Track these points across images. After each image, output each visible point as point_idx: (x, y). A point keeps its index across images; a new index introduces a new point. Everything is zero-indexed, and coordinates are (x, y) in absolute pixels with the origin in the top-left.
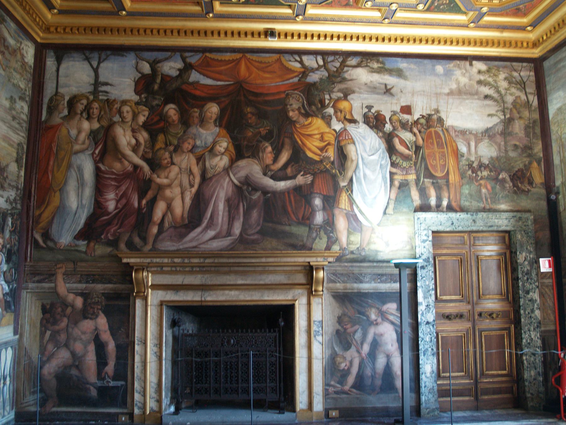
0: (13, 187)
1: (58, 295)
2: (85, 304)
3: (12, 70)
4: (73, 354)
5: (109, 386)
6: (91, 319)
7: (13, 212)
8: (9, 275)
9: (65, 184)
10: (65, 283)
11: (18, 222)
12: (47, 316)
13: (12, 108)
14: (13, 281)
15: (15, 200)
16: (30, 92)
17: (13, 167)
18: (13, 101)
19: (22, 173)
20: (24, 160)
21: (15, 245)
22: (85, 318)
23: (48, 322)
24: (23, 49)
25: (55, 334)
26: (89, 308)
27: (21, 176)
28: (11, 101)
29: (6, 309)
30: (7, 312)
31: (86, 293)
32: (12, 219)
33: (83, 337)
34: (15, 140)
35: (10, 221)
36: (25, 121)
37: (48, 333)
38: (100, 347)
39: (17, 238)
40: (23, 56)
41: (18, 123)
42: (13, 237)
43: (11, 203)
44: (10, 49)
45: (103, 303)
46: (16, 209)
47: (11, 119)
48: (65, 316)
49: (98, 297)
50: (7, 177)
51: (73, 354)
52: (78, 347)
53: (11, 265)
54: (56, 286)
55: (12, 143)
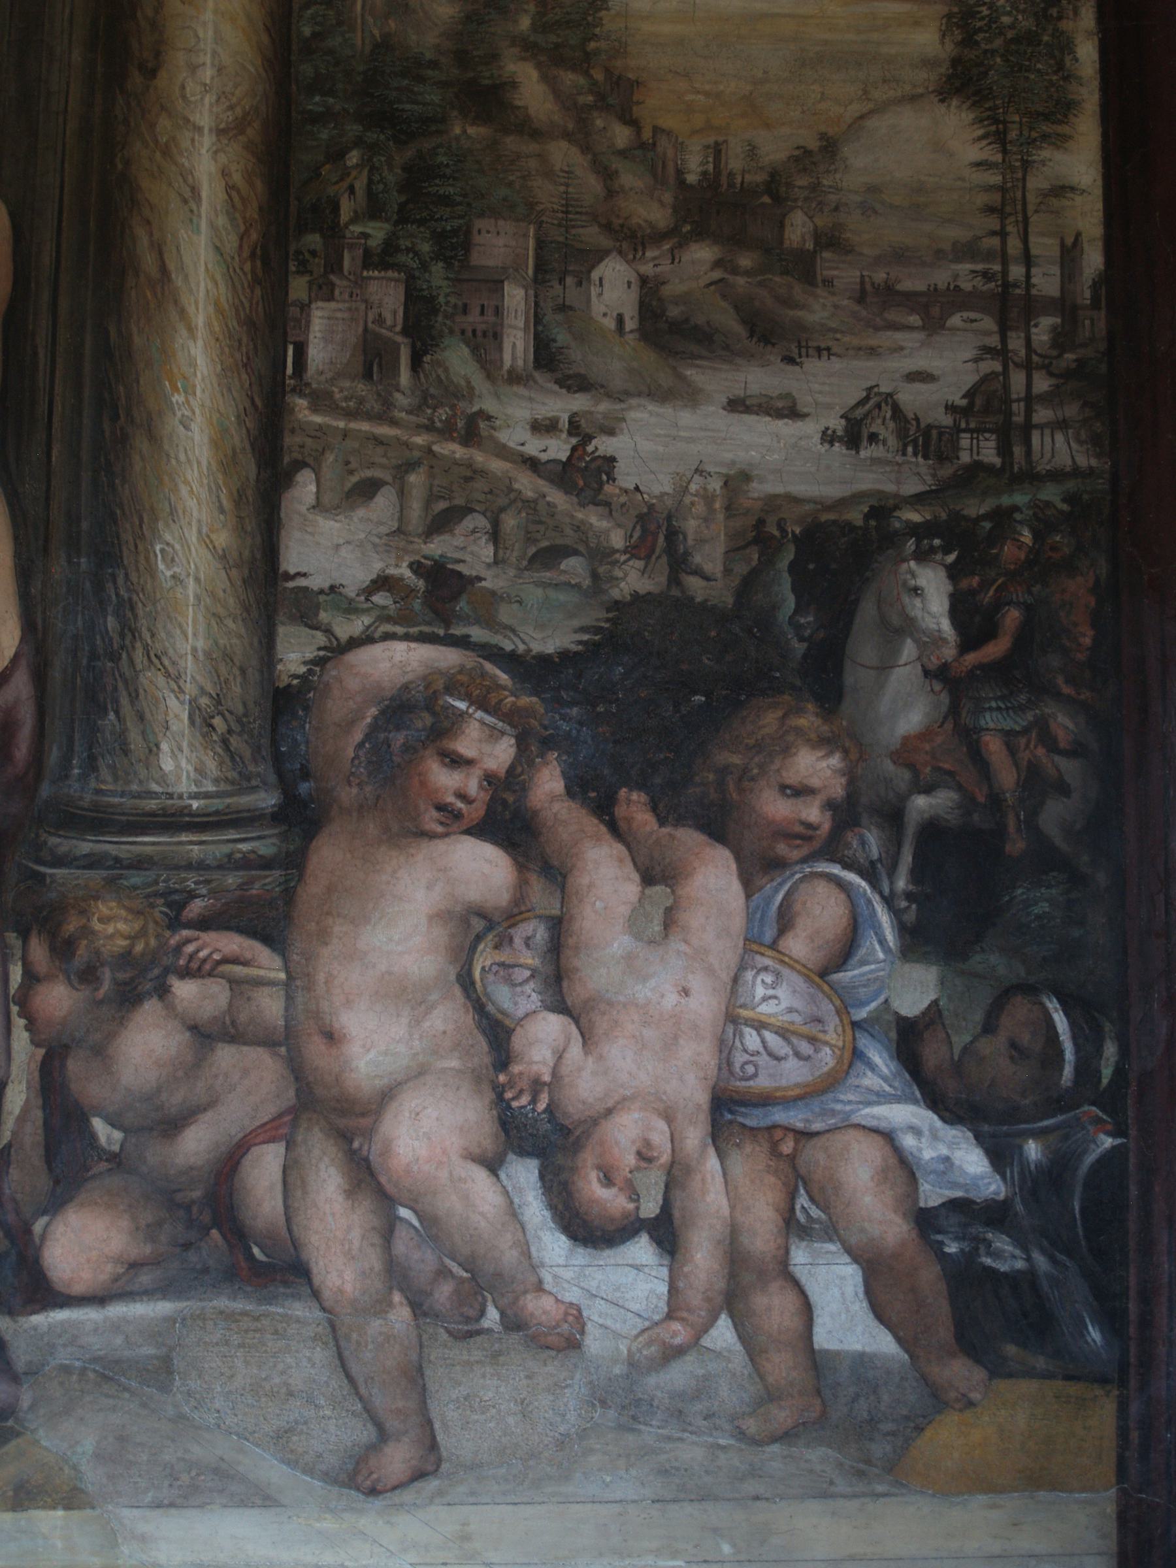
0: (933, 311)
7: (975, 507)
8: (993, 1047)
11: (1077, 592)
14: (1059, 1103)
15: (985, 406)
17: (929, 149)
19: (1077, 162)
20: (1087, 53)
21: (1036, 783)
27: (1062, 190)
29: (971, 1341)
30: (998, 1370)
32: (954, 573)
39: (1064, 724)
42: (989, 720)
46: (1030, 477)
50: (830, 240)
53: (993, 961)
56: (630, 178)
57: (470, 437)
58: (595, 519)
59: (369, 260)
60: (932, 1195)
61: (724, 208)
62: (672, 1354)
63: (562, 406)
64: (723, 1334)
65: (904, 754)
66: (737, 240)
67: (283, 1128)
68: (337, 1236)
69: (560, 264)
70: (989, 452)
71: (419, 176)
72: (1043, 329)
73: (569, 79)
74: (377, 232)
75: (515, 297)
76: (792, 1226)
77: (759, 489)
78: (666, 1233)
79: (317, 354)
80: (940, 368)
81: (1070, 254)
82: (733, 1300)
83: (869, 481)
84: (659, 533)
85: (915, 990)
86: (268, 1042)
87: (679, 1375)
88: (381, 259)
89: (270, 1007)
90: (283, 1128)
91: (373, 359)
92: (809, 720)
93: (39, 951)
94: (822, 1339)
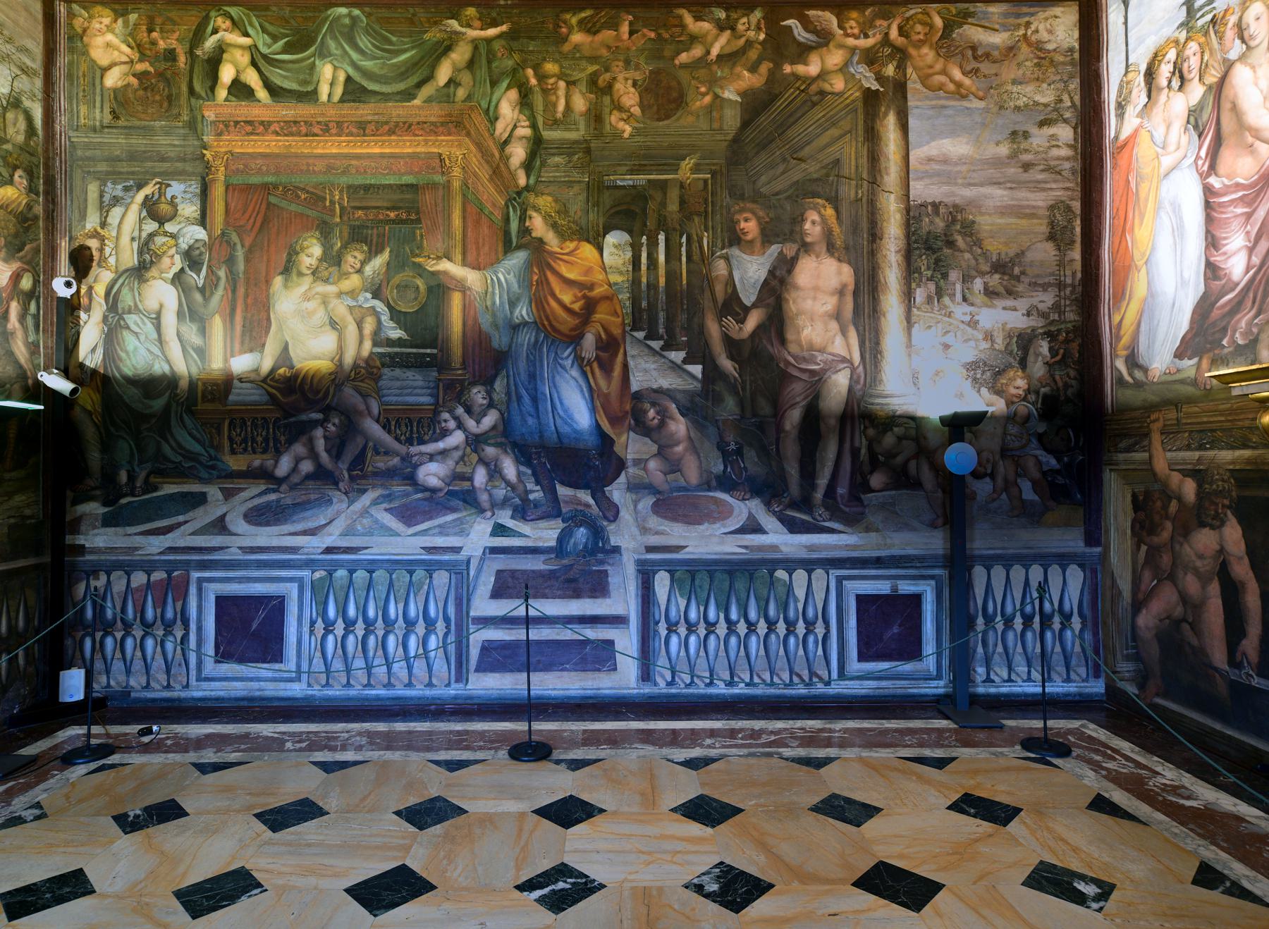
0: (1045, 287)
1: (1155, 475)
2: (1200, 494)
3: (1009, 87)
4: (1184, 599)
5: (1250, 686)
6: (1212, 527)
7: (1053, 329)
9: (1153, 249)
10: (1164, 450)
11: (1075, 346)
12: (1142, 515)
13: (1013, 155)
15: (1056, 307)
16: (1077, 98)
17: (1044, 252)
18: (1020, 139)
19: (1076, 254)
20: (1078, 230)
21: (1066, 386)
22: (1203, 525)
23: (1142, 527)
24: (1037, 31)
25: (1153, 552)
26: (1207, 504)
27: (1072, 260)
28: (1013, 141)
31: (1200, 471)
33: (1199, 563)
34: (1040, 204)
35: (1044, 347)
36: (1068, 159)
37: (1144, 548)
38: (1232, 592)
39: (1072, 373)
40: (1038, 46)
41: (1043, 171)
43: (1043, 315)
44: (996, 53)
45: (1234, 494)
46: (1065, 322)
47: (1021, 170)
48: (1167, 517)
49: (1223, 480)
50: (1023, 273)
51: (1184, 599)
52: (1191, 584)
54: (1150, 457)
55: (1028, 211)
56: (981, 260)
57: (949, 316)
58: (975, 332)
59: (928, 280)
60: (1045, 468)
61: (999, 267)
62: (994, 500)
63: (968, 309)
64: (1004, 496)
65: (1039, 380)
66: (1004, 274)
67: (916, 457)
68: (927, 477)
69: (967, 279)
70: (1056, 317)
71: (937, 261)
72: (1068, 290)
73: (968, 239)
74: (929, 273)
75: (958, 287)
76: (1018, 475)
77: (1009, 326)
78: (992, 476)
79: (918, 300)
80: (1046, 299)
81: (1074, 274)
82: (1006, 489)
83: (1033, 324)
84: (989, 336)
85: (1041, 428)
86: (912, 439)
87: (995, 504)
88: (930, 279)
89: (913, 432)
90: (916, 457)
91: (929, 300)
92: (1020, 373)
93: (867, 423)
94: (1024, 496)
